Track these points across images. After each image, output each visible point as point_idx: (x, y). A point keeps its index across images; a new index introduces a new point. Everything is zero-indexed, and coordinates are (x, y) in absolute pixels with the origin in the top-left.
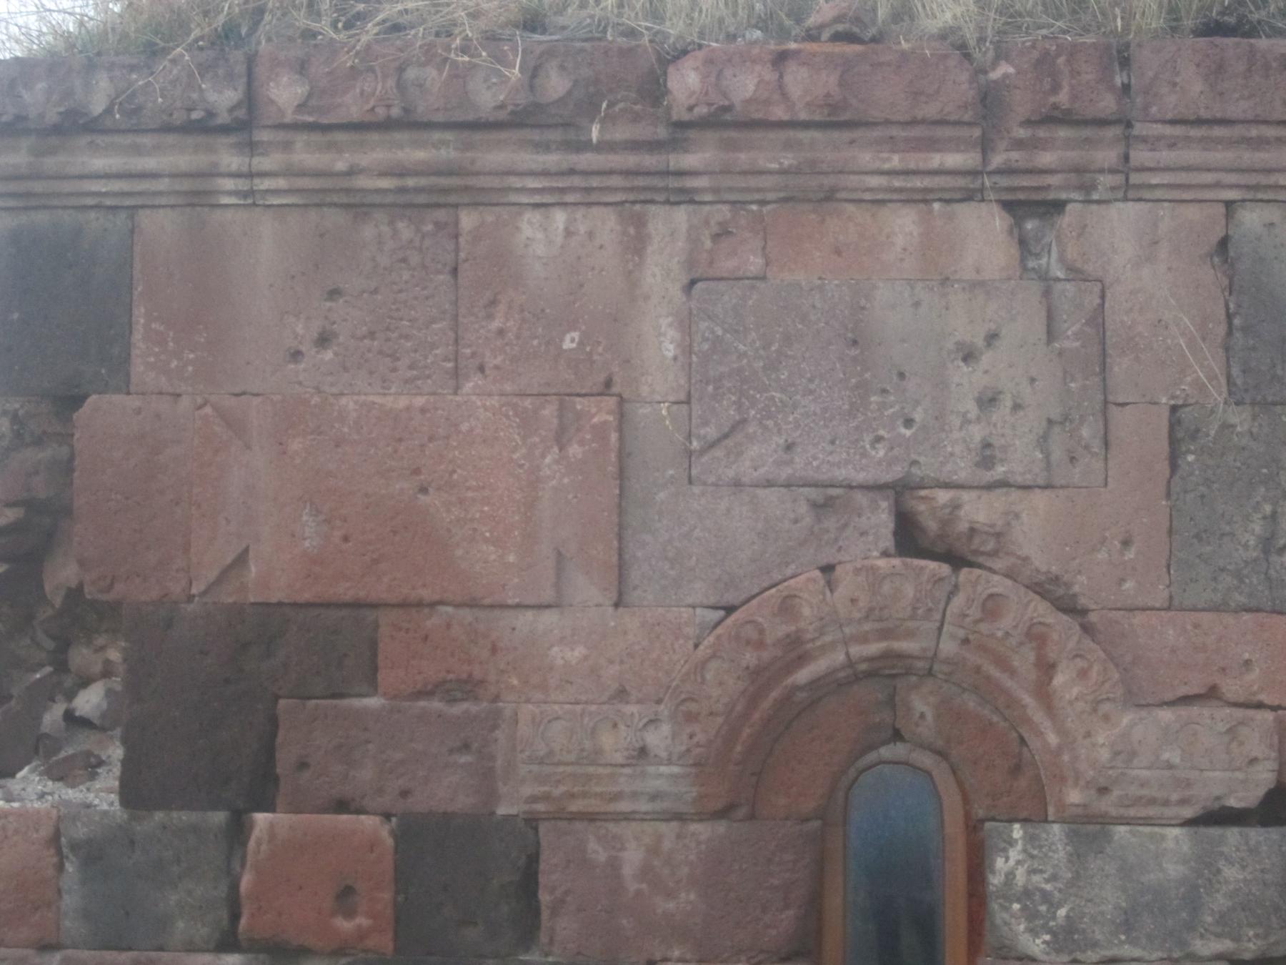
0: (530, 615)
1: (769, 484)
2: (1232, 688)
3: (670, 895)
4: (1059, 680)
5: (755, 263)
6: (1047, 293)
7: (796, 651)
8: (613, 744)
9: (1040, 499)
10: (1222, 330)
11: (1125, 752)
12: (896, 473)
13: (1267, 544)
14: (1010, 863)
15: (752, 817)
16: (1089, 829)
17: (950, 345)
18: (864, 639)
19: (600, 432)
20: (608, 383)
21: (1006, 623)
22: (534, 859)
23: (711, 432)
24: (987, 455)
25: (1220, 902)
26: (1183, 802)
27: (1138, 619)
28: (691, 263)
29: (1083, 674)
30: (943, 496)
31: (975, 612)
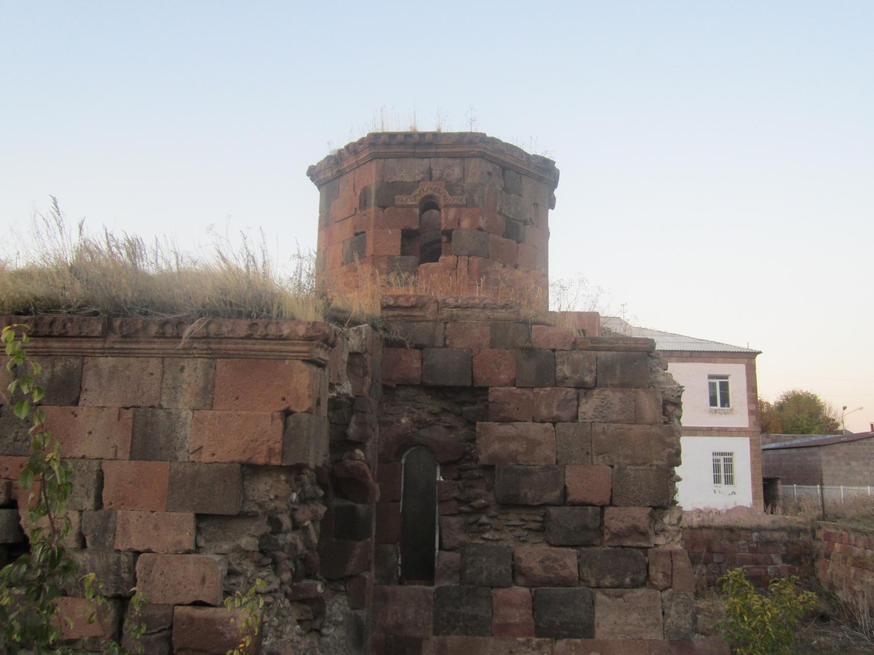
13: (15, 440)
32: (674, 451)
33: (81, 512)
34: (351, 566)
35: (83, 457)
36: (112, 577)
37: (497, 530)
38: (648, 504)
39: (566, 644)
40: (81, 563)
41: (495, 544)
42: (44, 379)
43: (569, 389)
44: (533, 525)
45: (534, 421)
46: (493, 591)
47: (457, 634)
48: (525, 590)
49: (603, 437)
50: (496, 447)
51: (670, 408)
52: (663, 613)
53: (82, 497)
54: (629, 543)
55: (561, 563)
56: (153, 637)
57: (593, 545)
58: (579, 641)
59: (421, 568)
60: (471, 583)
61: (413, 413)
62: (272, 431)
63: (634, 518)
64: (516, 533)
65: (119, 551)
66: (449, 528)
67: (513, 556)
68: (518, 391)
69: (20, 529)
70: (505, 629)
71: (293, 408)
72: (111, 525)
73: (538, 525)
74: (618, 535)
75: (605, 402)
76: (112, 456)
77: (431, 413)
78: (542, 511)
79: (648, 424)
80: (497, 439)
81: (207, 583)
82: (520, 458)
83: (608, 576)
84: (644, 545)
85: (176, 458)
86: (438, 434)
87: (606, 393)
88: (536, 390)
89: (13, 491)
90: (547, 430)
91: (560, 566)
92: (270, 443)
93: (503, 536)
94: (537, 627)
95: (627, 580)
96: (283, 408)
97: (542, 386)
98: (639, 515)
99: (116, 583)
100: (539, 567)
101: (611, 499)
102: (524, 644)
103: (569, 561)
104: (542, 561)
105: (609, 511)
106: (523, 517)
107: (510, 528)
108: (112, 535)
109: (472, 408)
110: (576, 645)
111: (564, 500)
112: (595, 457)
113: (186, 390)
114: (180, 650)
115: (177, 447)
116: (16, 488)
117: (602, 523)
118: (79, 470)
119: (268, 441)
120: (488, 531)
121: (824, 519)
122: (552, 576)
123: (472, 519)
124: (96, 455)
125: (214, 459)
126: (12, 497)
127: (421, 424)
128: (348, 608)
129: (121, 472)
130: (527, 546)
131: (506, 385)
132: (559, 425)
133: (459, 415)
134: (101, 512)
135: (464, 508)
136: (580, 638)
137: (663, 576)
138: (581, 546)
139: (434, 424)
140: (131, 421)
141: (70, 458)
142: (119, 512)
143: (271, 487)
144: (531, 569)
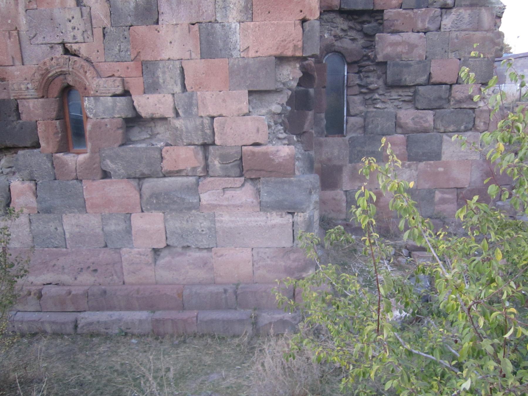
0: (11, 67)
1: (42, 44)
2: (116, 74)
3: (37, 110)
4: (87, 74)
5: (35, 6)
6: (81, 9)
7: (48, 71)
8: (23, 87)
9: (84, 44)
10: (109, 14)
11: (98, 85)
12: (61, 41)
13: (120, 51)
14: (86, 103)
15: (47, 98)
16: (96, 97)
17: (66, 19)
18: (58, 68)
19: (15, 36)
20: (16, 28)
21: (78, 65)
22: (18, 106)
23: (32, 36)
24: (74, 37)
25: (117, 109)
26: (109, 93)
27: (101, 64)
28: (25, 7)
29: (91, 73)
30: (69, 45)
31: (73, 63)
32: (499, 48)
33: (173, 94)
34: (306, 127)
35: (169, 59)
36: (200, 133)
37: (383, 102)
38: (480, 82)
39: (425, 164)
40: (179, 126)
41: (382, 110)
42: (131, 7)
43: (436, 9)
44: (407, 98)
45: (413, 31)
48: (402, 136)
49: (456, 41)
50: (389, 50)
51: (498, 20)
52: (481, 145)
53: (172, 85)
54: (465, 106)
55: (424, 119)
56: (229, 165)
57: (443, 108)
58: (432, 162)
59: (336, 126)
60: (372, 133)
61: (331, 30)
62: (296, 32)
64: (395, 104)
65: (202, 117)
66: (356, 103)
67: (396, 117)
68: (404, 11)
69: (134, 108)
71: (308, 17)
72: (194, 102)
73: (411, 98)
74: (459, 102)
75: (459, 17)
76: (188, 57)
77: (343, 30)
78: (412, 90)
79: (485, 31)
80: (387, 45)
81: (260, 132)
82: (404, 57)
83: (452, 126)
84: (474, 107)
85: (232, 56)
86: (346, 44)
87: (460, 11)
88: (415, 10)
89: (125, 84)
90: (421, 37)
91: (424, 121)
92: (294, 42)
93: (387, 106)
94: (409, 156)
95: (462, 127)
96: (301, 18)
97: (419, 7)
99: (202, 136)
100: (411, 122)
104: (413, 119)
105: (455, 87)
106: (400, 93)
108: (196, 108)
109: (370, 25)
110: (430, 164)
111: (429, 82)
112: (450, 54)
113: (233, 8)
114: (247, 171)
115: (232, 49)
116: (127, 83)
117: (450, 95)
118: (168, 68)
119: (293, 40)
120: (379, 103)
121: (520, 101)
122: (418, 127)
123: (367, 97)
124: (178, 57)
125: (258, 54)
126: (126, 89)
127: (337, 38)
128: (303, 151)
129: (196, 67)
130: (403, 111)
131: (395, 8)
132: (428, 34)
133: (361, 31)
134: (187, 93)
135: (364, 90)
136: (433, 160)
138: (436, 109)
139: (343, 38)
140: (198, 32)
141: (161, 60)
142: (199, 93)
143: (291, 72)
144: (407, 123)
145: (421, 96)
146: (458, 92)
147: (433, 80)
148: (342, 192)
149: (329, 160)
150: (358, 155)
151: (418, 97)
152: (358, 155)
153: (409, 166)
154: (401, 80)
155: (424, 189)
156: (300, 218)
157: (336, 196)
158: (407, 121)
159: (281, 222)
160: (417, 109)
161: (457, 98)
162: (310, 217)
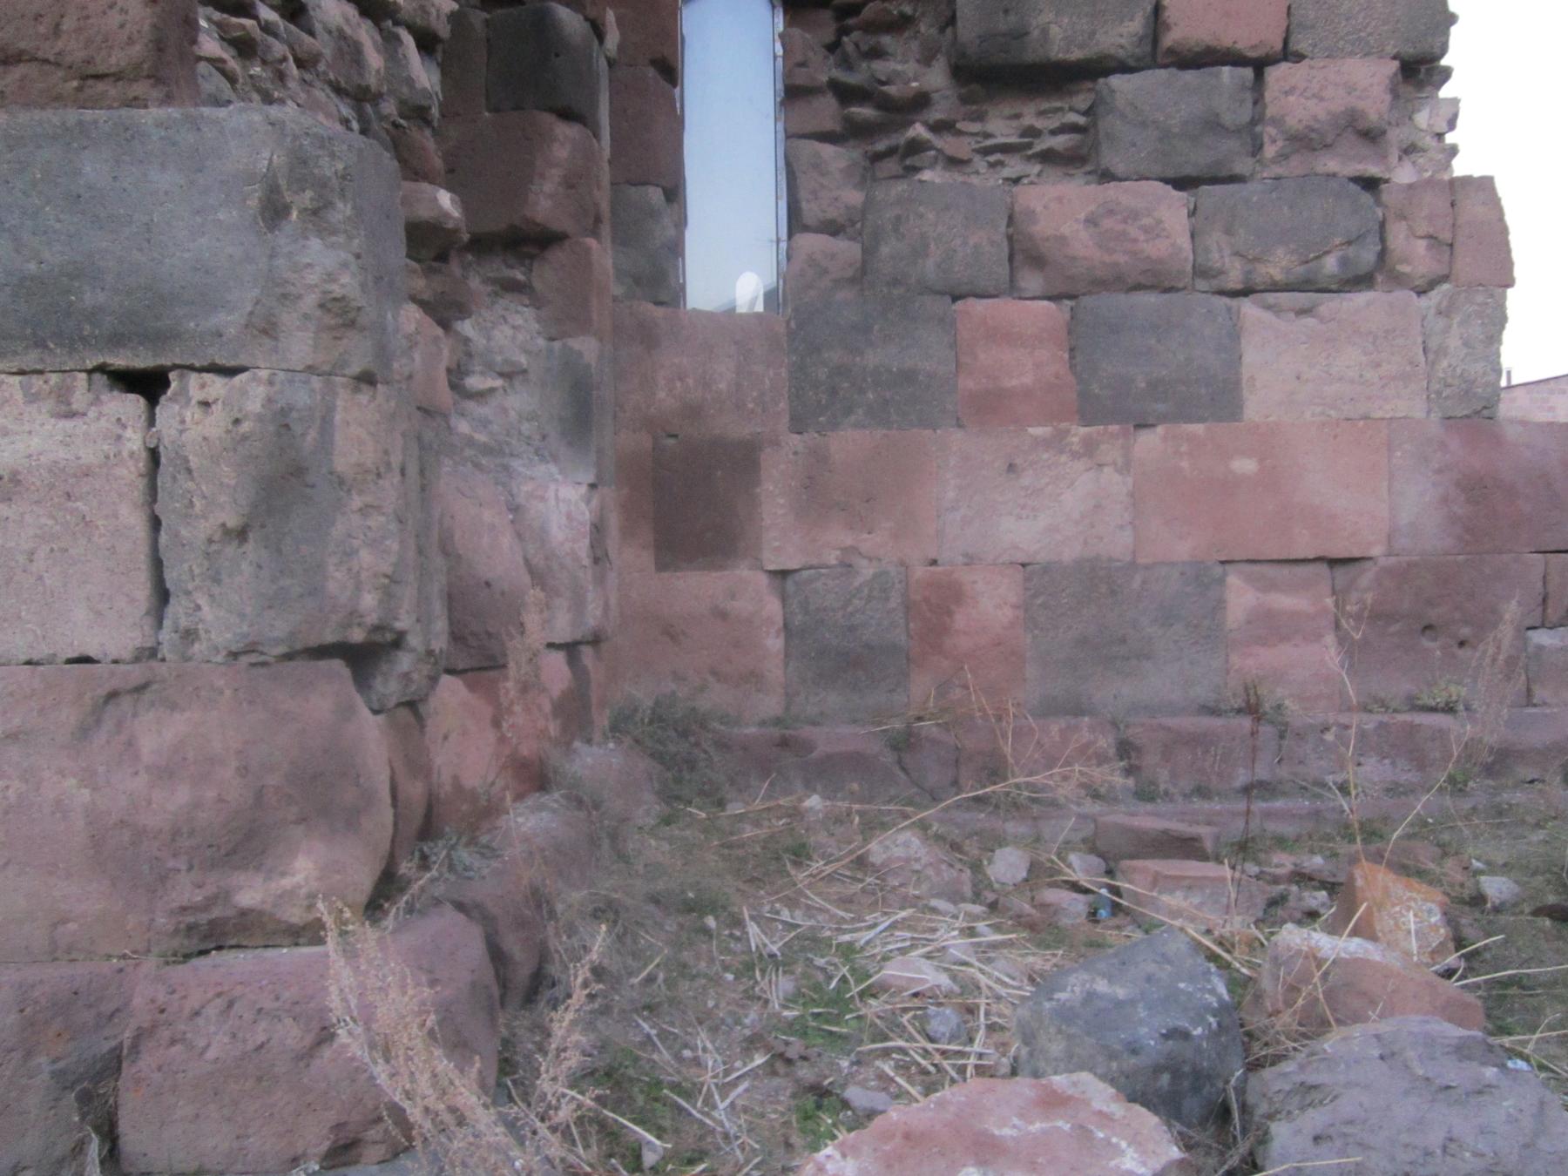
37: (954, 162)
38: (1391, 49)
39: (1165, 439)
44: (1060, 142)
46: (960, 305)
47: (857, 426)
55: (1146, 221)
58: (1198, 428)
60: (895, 282)
63: (1350, 89)
70: (991, 407)
74: (1304, 142)
91: (1146, 230)
95: (1330, 264)
98: (1367, 80)
100: (1084, 235)
101: (1286, 42)
102: (1046, 443)
103: (1166, 221)
104: (1091, 221)
105: (1274, 74)
106: (1029, 120)
107: (992, 158)
120: (932, 166)
122: (1122, 259)
128: (541, 342)
137: (1429, 248)
144: (1062, 240)
145: (1123, 116)
146: (1299, 95)
147: (1168, 40)
148: (764, 580)
149: (693, 412)
150: (833, 392)
151: (1108, 123)
152: (833, 392)
153: (1090, 447)
154: (1020, 35)
155: (1173, 564)
156: (196, 417)
157: (733, 597)
158: (1066, 230)
159: (62, 454)
160: (1106, 176)
161: (1292, 123)
162: (281, 420)
